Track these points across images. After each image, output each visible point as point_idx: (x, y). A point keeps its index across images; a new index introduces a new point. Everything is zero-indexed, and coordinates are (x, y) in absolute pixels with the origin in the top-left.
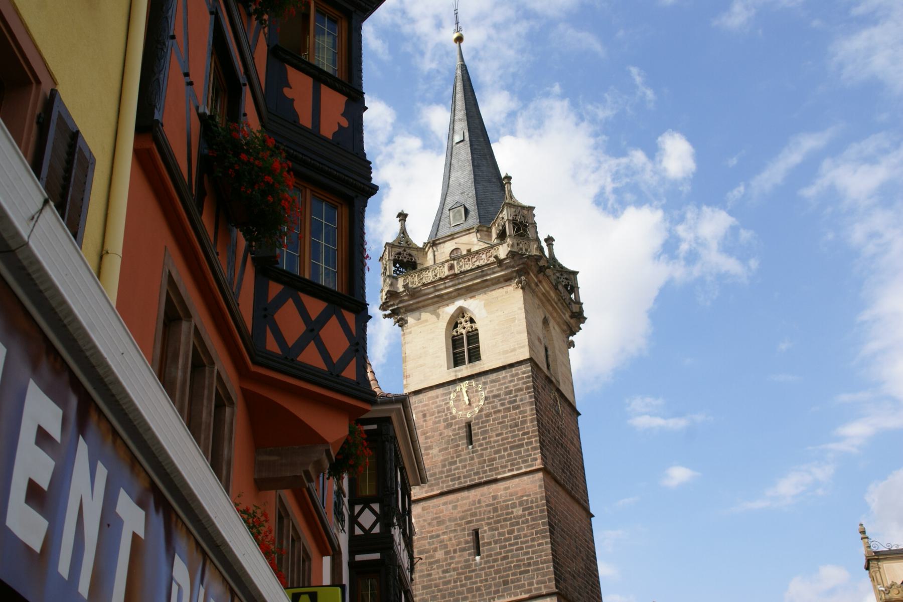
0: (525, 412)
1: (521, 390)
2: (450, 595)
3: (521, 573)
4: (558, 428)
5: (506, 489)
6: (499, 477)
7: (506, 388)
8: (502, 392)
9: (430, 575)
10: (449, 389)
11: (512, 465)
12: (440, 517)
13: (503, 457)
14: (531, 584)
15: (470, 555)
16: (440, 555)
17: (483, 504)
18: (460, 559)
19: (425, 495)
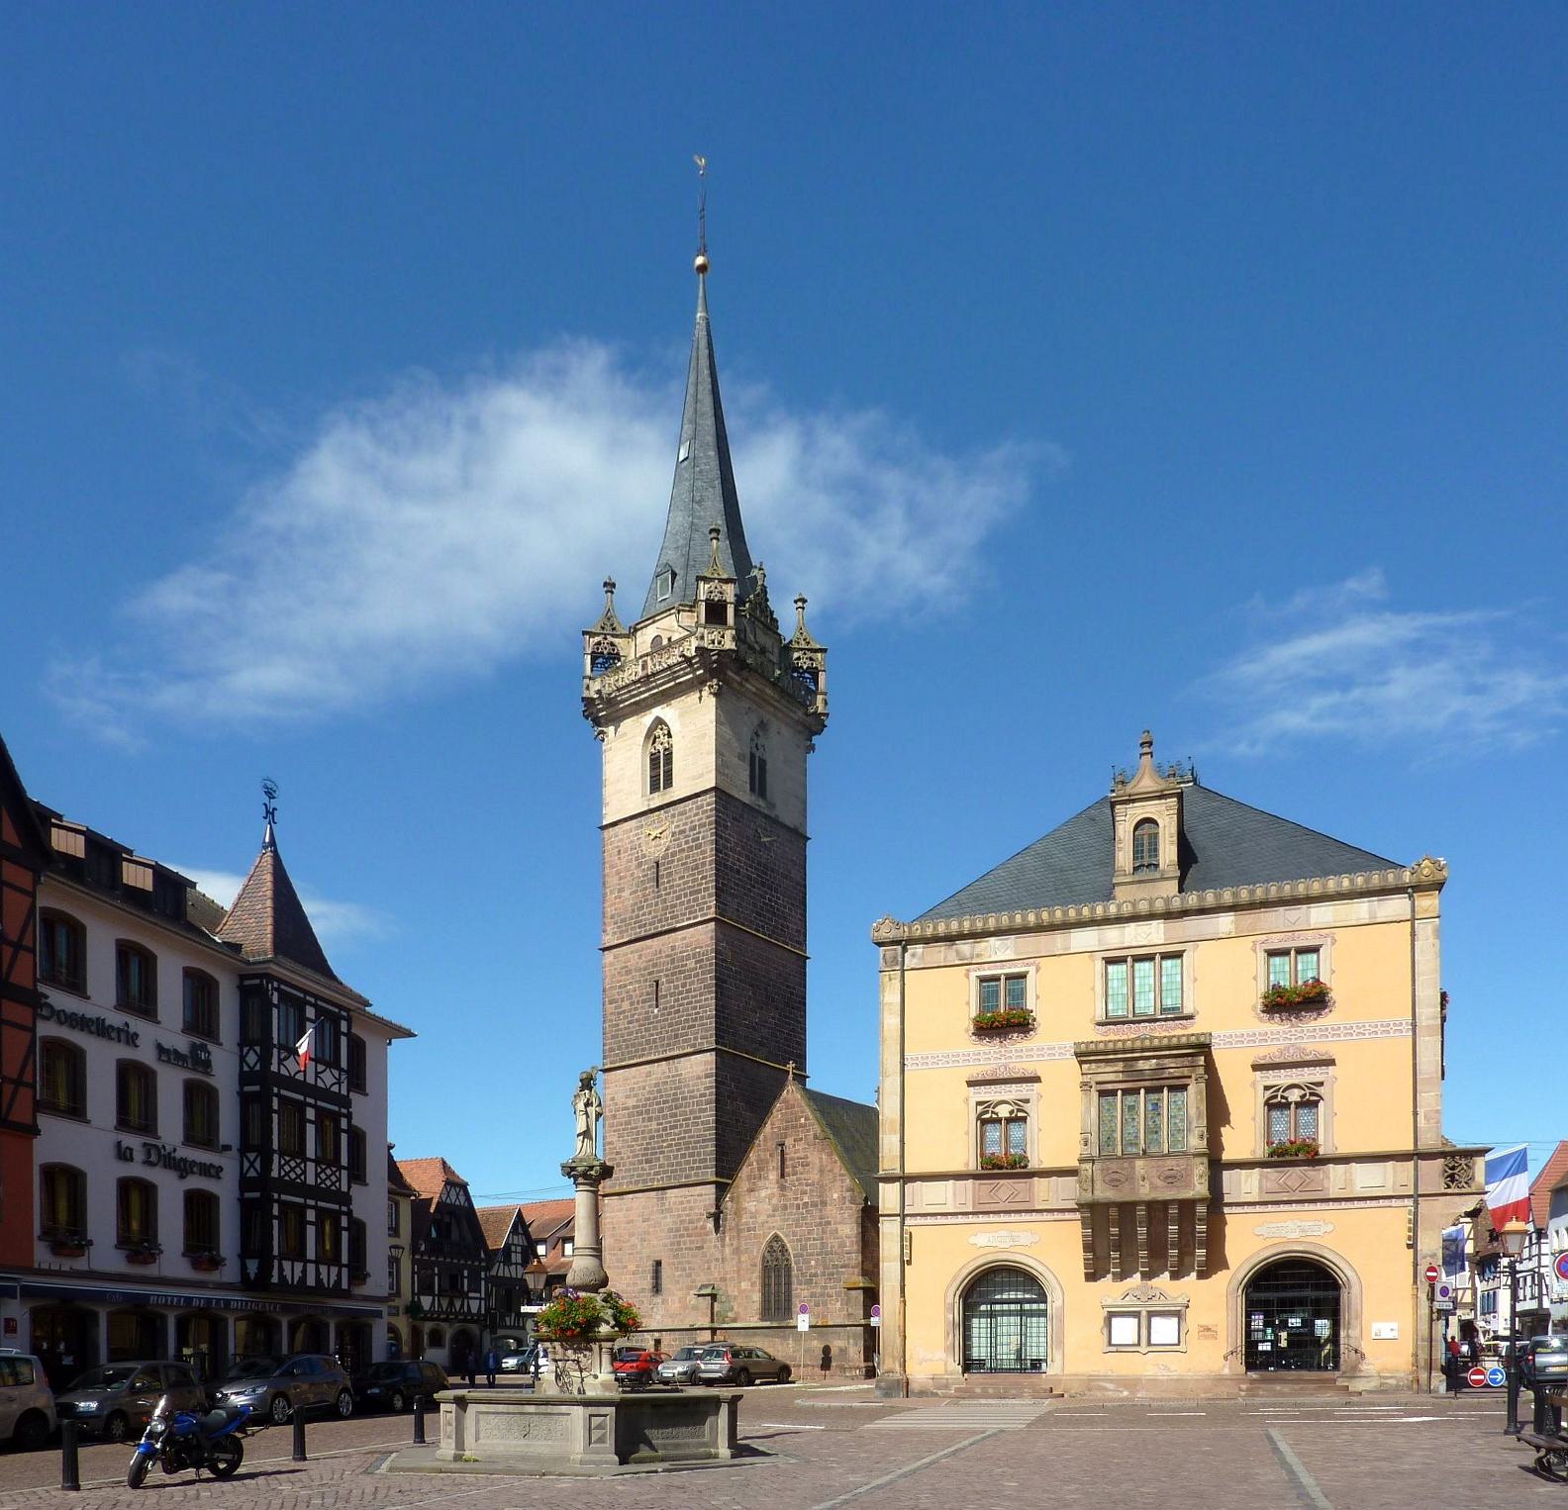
0: (704, 852)
1: (702, 825)
2: (633, 1045)
3: (690, 1027)
4: (759, 864)
5: (684, 938)
6: (678, 925)
7: (692, 822)
8: (687, 827)
9: (618, 1025)
10: (641, 822)
11: (690, 913)
12: (627, 967)
13: (682, 904)
14: (696, 1039)
15: (650, 1006)
16: (626, 1005)
17: (663, 955)
18: (642, 1009)
19: (616, 942)
